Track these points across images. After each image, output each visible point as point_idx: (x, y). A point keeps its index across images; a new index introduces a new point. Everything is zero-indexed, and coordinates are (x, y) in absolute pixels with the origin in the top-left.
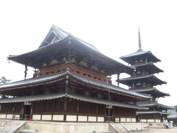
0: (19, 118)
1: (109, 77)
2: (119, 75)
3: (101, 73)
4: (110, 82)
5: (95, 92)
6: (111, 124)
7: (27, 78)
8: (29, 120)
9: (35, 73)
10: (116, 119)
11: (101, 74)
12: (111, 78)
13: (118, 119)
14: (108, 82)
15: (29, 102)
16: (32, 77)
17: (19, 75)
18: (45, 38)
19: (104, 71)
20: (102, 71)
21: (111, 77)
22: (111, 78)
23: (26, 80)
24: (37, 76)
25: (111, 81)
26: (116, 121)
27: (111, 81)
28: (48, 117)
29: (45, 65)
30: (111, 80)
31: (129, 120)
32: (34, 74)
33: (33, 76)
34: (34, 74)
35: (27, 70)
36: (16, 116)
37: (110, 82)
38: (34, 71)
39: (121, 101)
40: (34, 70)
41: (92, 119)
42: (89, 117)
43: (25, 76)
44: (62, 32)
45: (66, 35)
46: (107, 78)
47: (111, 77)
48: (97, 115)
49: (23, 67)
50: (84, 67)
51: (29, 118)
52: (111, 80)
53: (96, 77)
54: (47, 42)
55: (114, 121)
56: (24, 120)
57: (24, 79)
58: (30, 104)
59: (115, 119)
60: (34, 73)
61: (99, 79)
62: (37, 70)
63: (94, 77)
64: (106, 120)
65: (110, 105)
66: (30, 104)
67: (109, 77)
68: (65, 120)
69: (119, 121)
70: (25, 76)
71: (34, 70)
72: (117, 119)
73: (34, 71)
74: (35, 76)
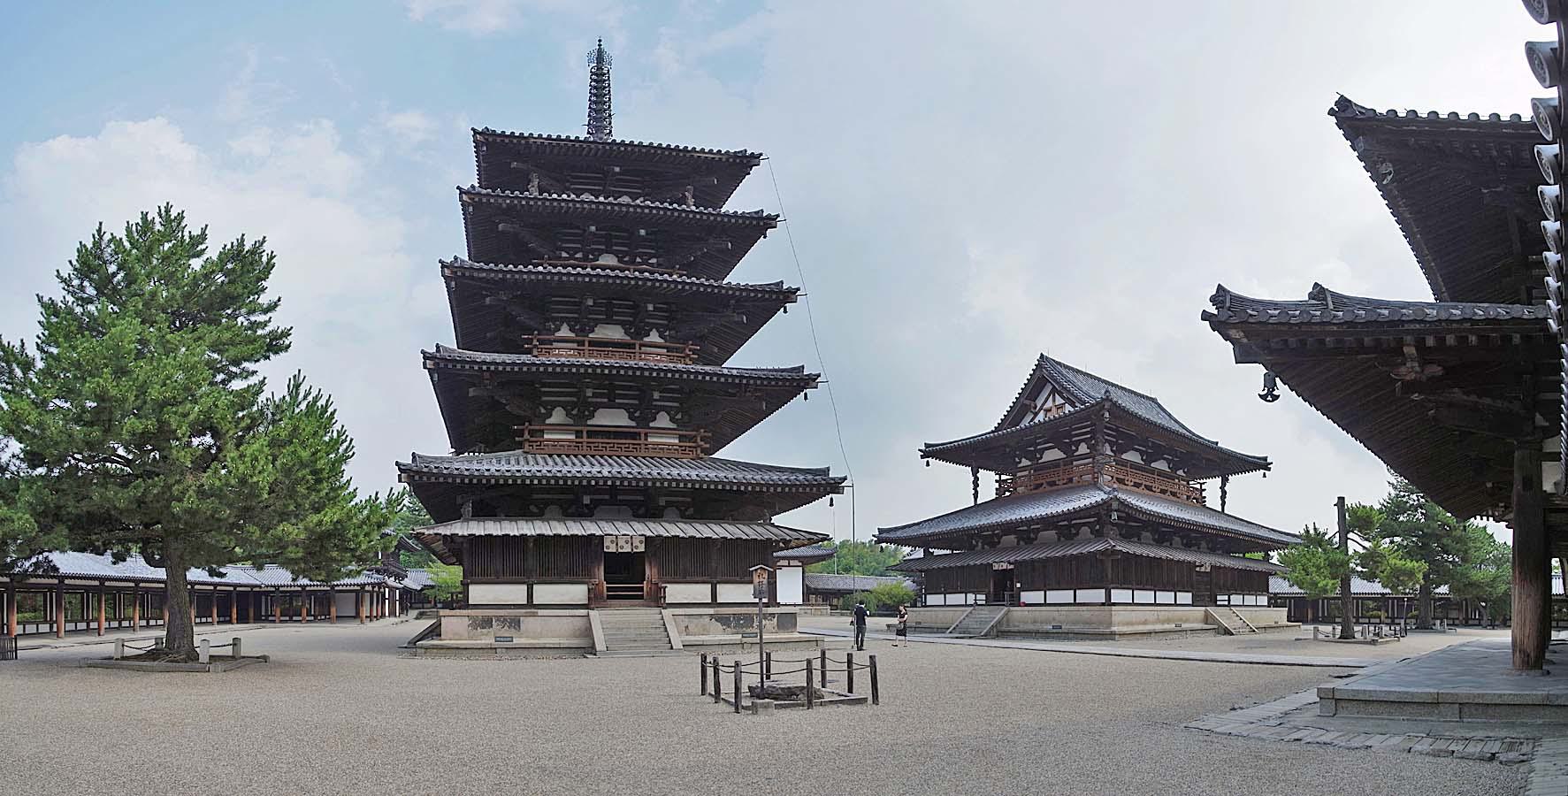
5: (1164, 531)
17: (954, 491)
20: (1180, 472)
23: (977, 508)
28: (1066, 596)
29: (1025, 462)
31: (1250, 600)
35: (976, 479)
37: (1201, 501)
39: (1227, 553)
41: (1166, 597)
44: (1070, 376)
45: (1099, 395)
48: (1175, 588)
50: (1134, 466)
51: (1016, 601)
55: (1214, 603)
65: (1206, 561)
68: (1108, 603)
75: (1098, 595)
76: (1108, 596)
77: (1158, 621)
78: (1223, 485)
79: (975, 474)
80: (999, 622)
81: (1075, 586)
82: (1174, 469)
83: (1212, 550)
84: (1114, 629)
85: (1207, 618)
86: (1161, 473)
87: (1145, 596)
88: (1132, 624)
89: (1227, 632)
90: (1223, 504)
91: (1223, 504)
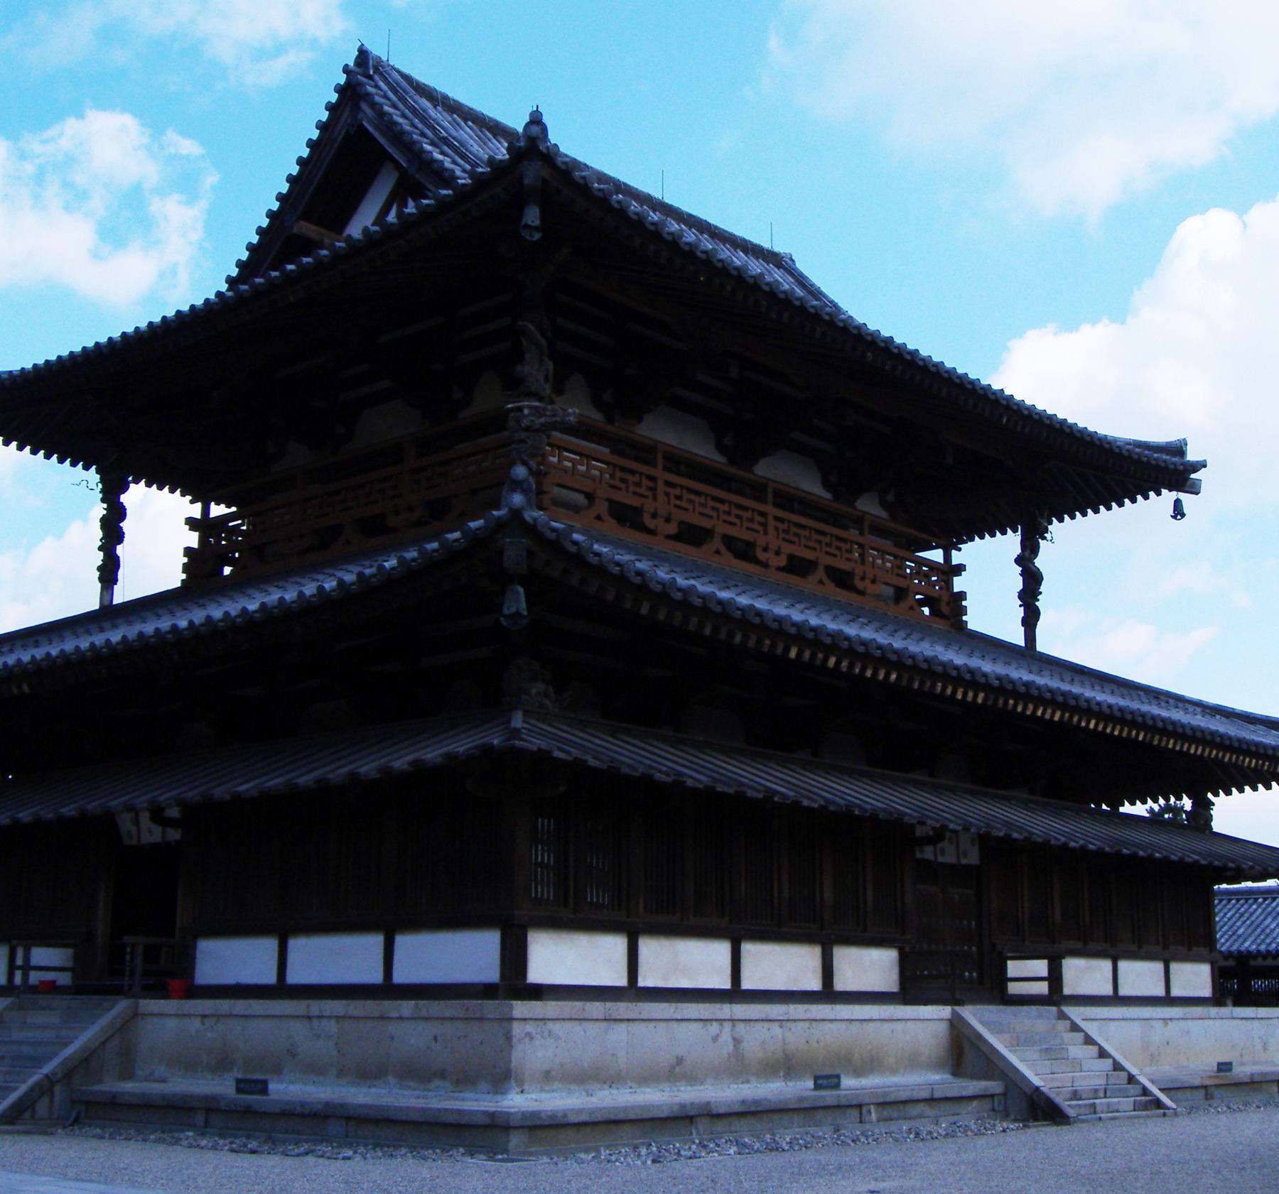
0: (64, 979)
1: (936, 555)
2: (1042, 532)
3: (859, 521)
4: (945, 609)
6: (973, 1015)
7: (123, 593)
8: (159, 989)
9: (202, 540)
10: (1015, 968)
11: (853, 534)
12: (960, 569)
13: (1040, 967)
14: (926, 611)
15: (157, 815)
16: (171, 576)
18: (285, 188)
19: (883, 504)
20: (869, 506)
21: (957, 557)
22: (960, 569)
23: (108, 613)
24: (227, 570)
25: (962, 595)
26: (1013, 988)
27: (962, 595)
28: (346, 957)
30: (959, 584)
31: (1141, 976)
32: (188, 551)
33: (186, 568)
34: (188, 551)
36: (41, 955)
37: (950, 608)
38: (192, 523)
40: (196, 511)
42: (748, 948)
43: (109, 572)
46: (917, 573)
47: (957, 557)
48: (826, 929)
49: (79, 485)
51: (173, 977)
52: (959, 584)
53: (809, 555)
54: (306, 228)
55: (994, 989)
56: (118, 991)
57: (90, 601)
58: (174, 835)
59: (1004, 969)
60: (196, 546)
61: (842, 579)
62: (217, 510)
63: (791, 558)
64: (912, 988)
66: (174, 835)
67: (936, 555)
68: (514, 982)
69: (1042, 988)
70: (109, 572)
71: (196, 511)
72: (1027, 972)
73: (192, 523)
74: (199, 564)
75: (470, 954)
76: (515, 958)
77: (738, 1067)
78: (1026, 561)
79: (112, 493)
80: (86, 1063)
81: (393, 911)
82: (846, 483)
83: (993, 777)
84: (516, 1101)
85: (963, 1051)
86: (788, 500)
87: (697, 961)
88: (614, 1079)
89: (1041, 1109)
90: (1031, 618)
91: (1031, 618)
